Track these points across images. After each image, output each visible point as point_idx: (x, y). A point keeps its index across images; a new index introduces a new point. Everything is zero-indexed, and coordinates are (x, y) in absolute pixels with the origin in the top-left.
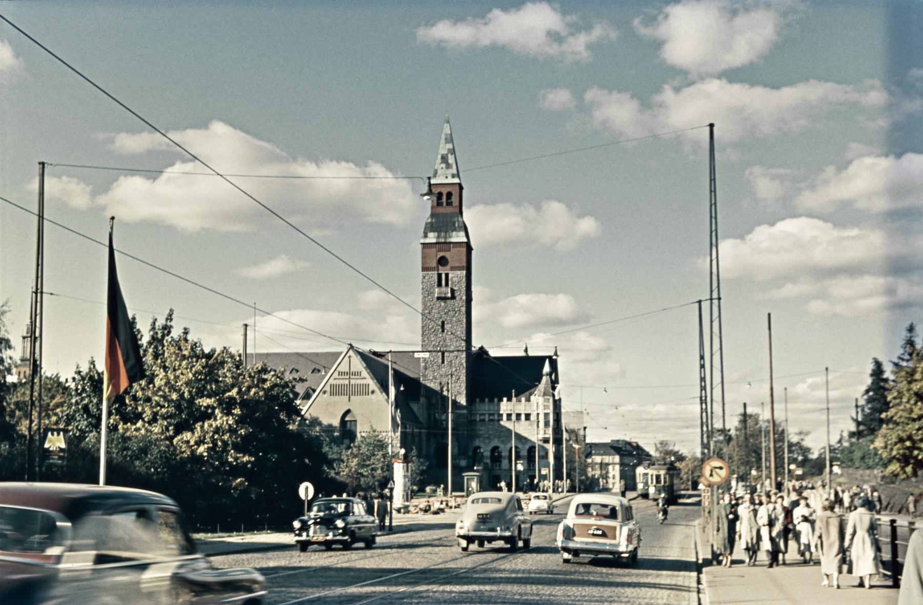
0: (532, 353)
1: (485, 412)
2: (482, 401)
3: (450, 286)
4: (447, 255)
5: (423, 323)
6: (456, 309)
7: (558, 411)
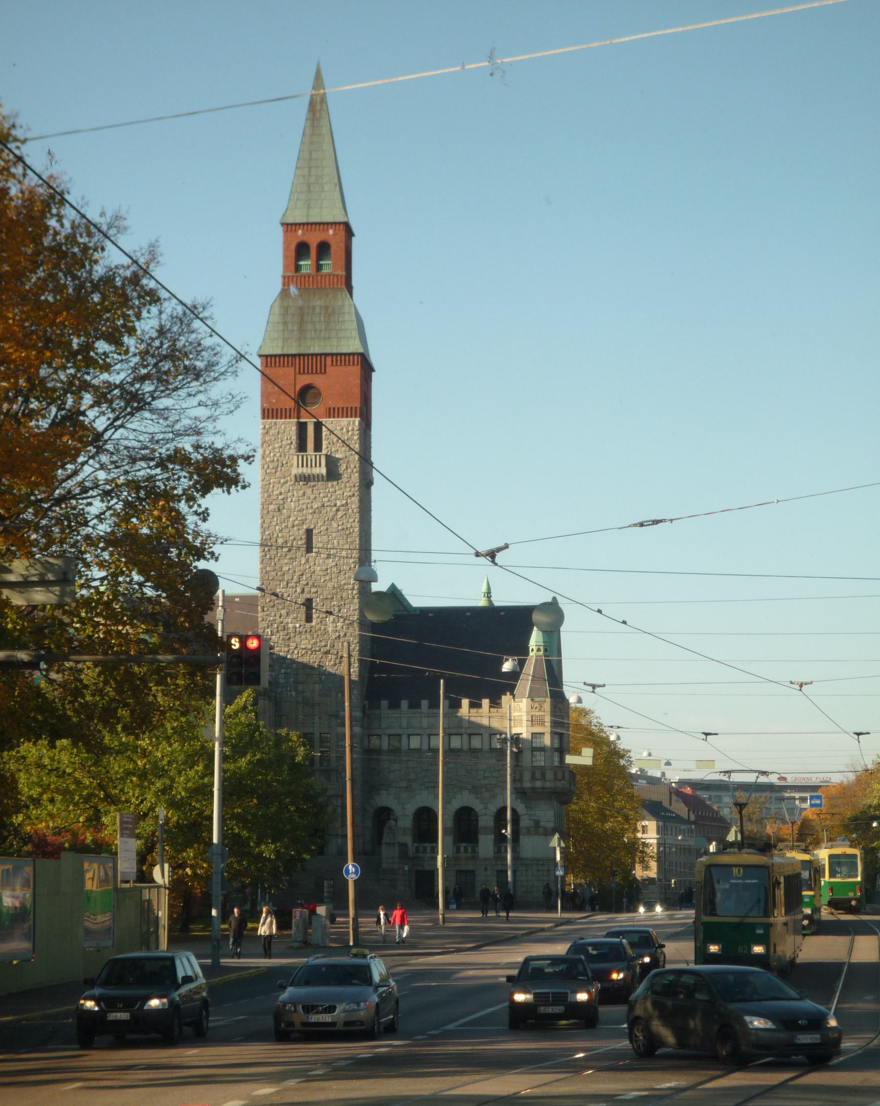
0: (501, 600)
1: (399, 731)
2: (395, 705)
3: (324, 451)
4: (317, 380)
5: (263, 533)
6: (338, 503)
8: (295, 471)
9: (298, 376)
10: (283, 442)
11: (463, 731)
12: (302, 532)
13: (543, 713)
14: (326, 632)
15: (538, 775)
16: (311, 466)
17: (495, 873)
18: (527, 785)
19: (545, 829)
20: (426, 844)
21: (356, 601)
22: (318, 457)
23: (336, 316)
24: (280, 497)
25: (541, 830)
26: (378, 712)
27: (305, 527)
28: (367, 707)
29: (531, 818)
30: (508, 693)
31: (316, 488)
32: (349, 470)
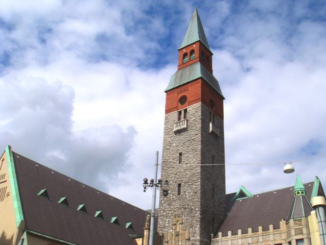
8: (175, 129)
13: (301, 227)
26: (217, 239)
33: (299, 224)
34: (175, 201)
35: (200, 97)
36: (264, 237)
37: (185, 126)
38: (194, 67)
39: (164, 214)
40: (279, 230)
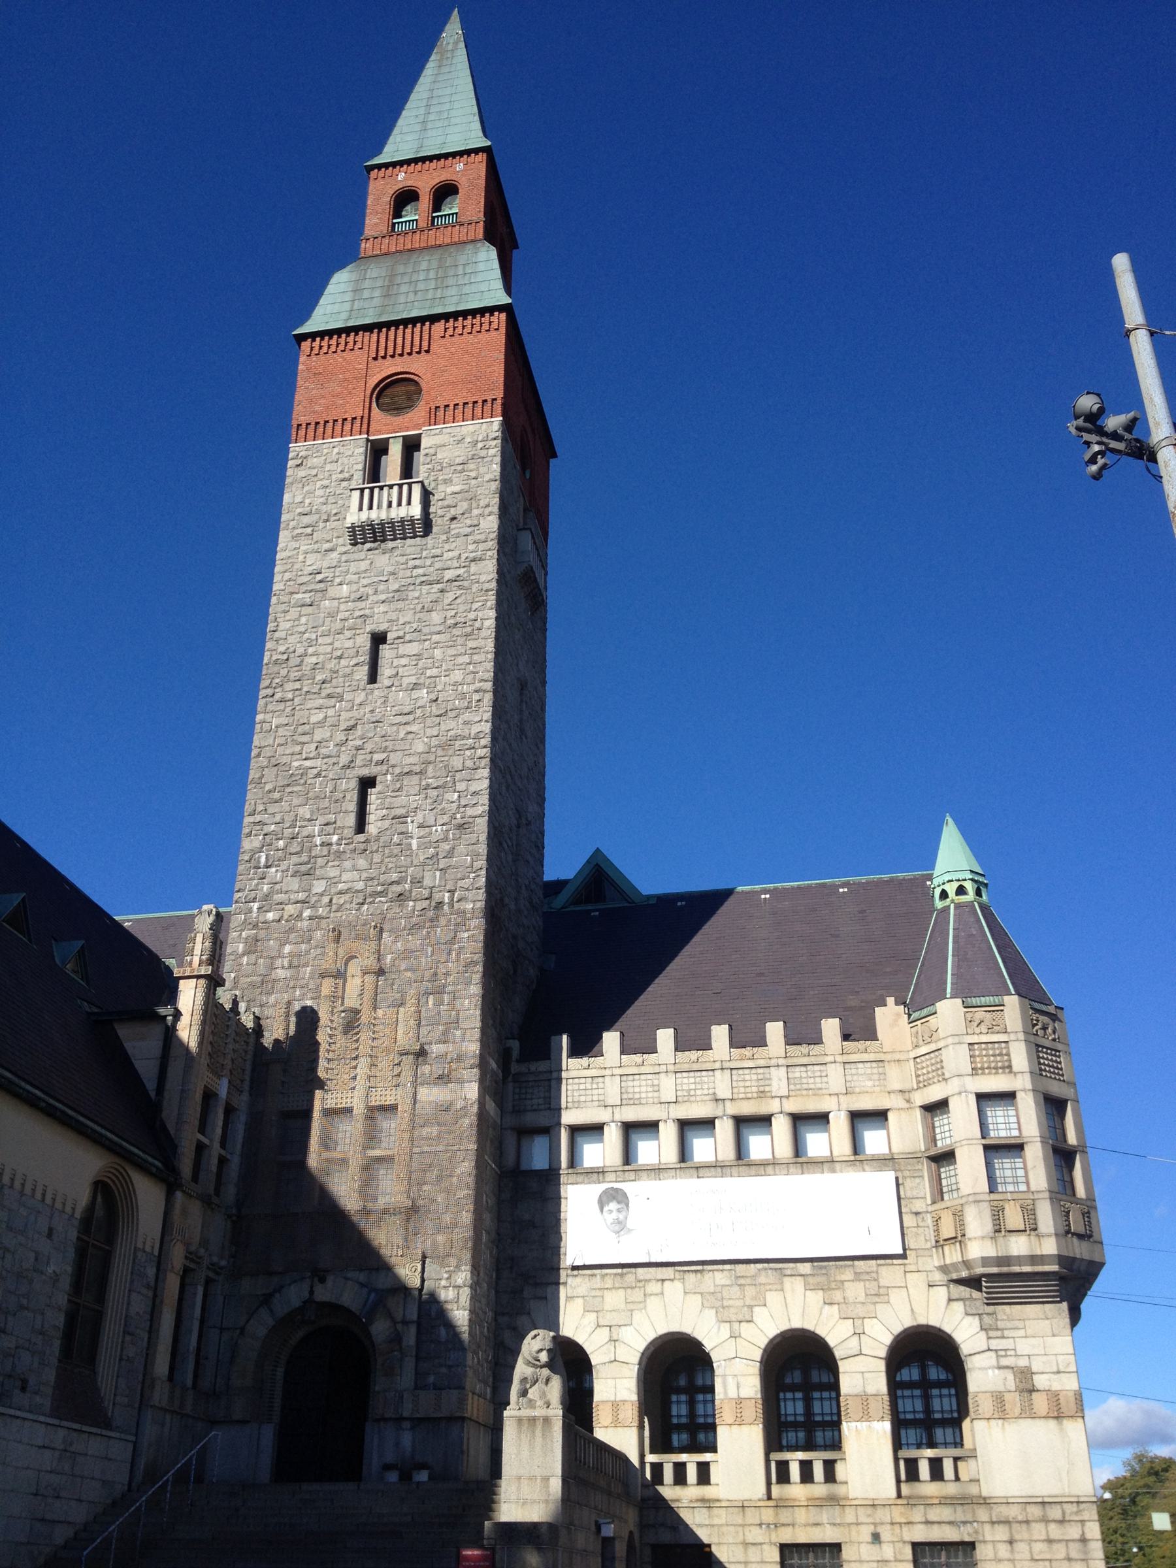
6: (449, 575)
7: (1057, 1089)
8: (354, 517)
9: (373, 363)
10: (334, 477)
11: (772, 1106)
12: (364, 642)
14: (404, 847)
15: (1013, 1218)
16: (390, 505)
17: (908, 1552)
18: (979, 1249)
19: (1054, 1397)
20: (683, 1457)
21: (485, 772)
22: (405, 487)
23: (461, 268)
24: (319, 577)
25: (1040, 1403)
26: (542, 1066)
27: (368, 629)
28: (515, 1054)
29: (1004, 1362)
30: (891, 1000)
31: (396, 553)
32: (475, 512)
33: (987, 1023)
34: (339, 855)
35: (499, 394)
36: (797, 1073)
37: (416, 511)
38: (462, 259)
39: (270, 916)
40: (816, 1049)
